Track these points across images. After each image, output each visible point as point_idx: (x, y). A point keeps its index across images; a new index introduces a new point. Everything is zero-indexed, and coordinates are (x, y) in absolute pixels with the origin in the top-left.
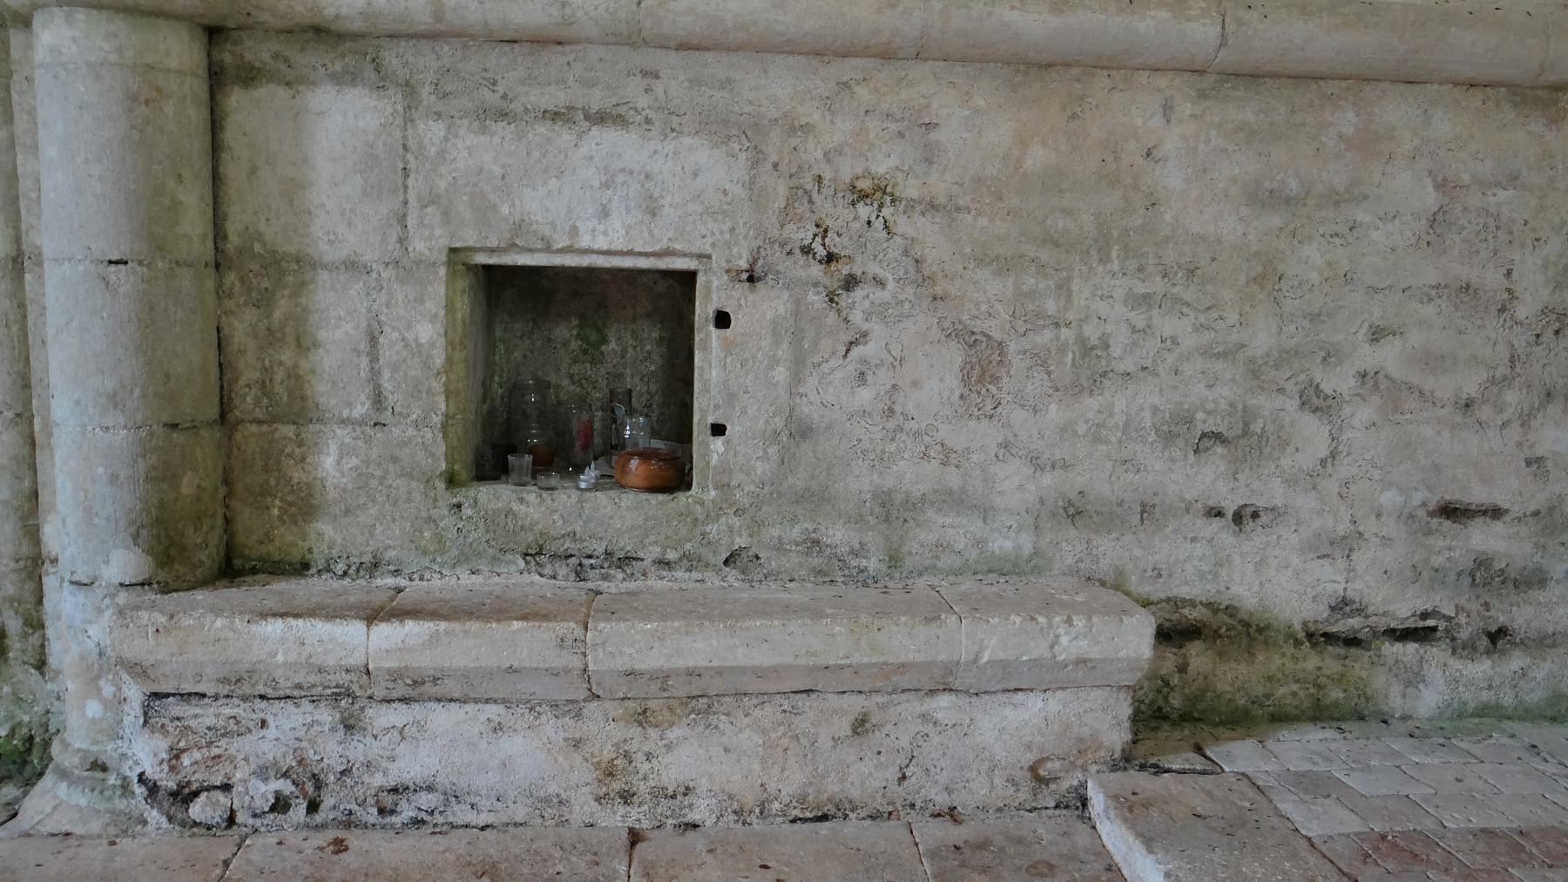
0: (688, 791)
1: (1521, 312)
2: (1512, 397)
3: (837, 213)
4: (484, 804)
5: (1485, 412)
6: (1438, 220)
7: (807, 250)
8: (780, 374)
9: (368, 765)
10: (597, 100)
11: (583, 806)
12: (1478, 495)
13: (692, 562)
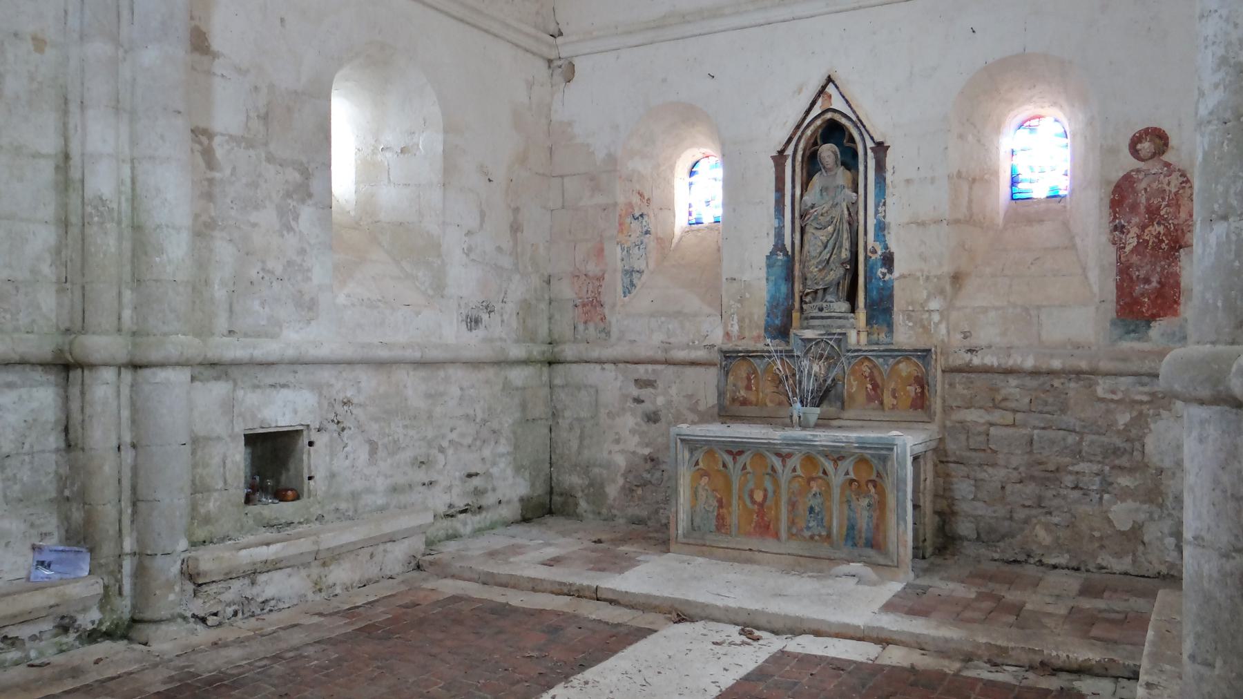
0: (335, 585)
1: (478, 420)
3: (341, 410)
4: (286, 601)
5: (473, 448)
6: (461, 398)
7: (333, 421)
8: (328, 458)
9: (257, 595)
10: (283, 381)
11: (310, 596)
12: (473, 471)
13: (307, 521)
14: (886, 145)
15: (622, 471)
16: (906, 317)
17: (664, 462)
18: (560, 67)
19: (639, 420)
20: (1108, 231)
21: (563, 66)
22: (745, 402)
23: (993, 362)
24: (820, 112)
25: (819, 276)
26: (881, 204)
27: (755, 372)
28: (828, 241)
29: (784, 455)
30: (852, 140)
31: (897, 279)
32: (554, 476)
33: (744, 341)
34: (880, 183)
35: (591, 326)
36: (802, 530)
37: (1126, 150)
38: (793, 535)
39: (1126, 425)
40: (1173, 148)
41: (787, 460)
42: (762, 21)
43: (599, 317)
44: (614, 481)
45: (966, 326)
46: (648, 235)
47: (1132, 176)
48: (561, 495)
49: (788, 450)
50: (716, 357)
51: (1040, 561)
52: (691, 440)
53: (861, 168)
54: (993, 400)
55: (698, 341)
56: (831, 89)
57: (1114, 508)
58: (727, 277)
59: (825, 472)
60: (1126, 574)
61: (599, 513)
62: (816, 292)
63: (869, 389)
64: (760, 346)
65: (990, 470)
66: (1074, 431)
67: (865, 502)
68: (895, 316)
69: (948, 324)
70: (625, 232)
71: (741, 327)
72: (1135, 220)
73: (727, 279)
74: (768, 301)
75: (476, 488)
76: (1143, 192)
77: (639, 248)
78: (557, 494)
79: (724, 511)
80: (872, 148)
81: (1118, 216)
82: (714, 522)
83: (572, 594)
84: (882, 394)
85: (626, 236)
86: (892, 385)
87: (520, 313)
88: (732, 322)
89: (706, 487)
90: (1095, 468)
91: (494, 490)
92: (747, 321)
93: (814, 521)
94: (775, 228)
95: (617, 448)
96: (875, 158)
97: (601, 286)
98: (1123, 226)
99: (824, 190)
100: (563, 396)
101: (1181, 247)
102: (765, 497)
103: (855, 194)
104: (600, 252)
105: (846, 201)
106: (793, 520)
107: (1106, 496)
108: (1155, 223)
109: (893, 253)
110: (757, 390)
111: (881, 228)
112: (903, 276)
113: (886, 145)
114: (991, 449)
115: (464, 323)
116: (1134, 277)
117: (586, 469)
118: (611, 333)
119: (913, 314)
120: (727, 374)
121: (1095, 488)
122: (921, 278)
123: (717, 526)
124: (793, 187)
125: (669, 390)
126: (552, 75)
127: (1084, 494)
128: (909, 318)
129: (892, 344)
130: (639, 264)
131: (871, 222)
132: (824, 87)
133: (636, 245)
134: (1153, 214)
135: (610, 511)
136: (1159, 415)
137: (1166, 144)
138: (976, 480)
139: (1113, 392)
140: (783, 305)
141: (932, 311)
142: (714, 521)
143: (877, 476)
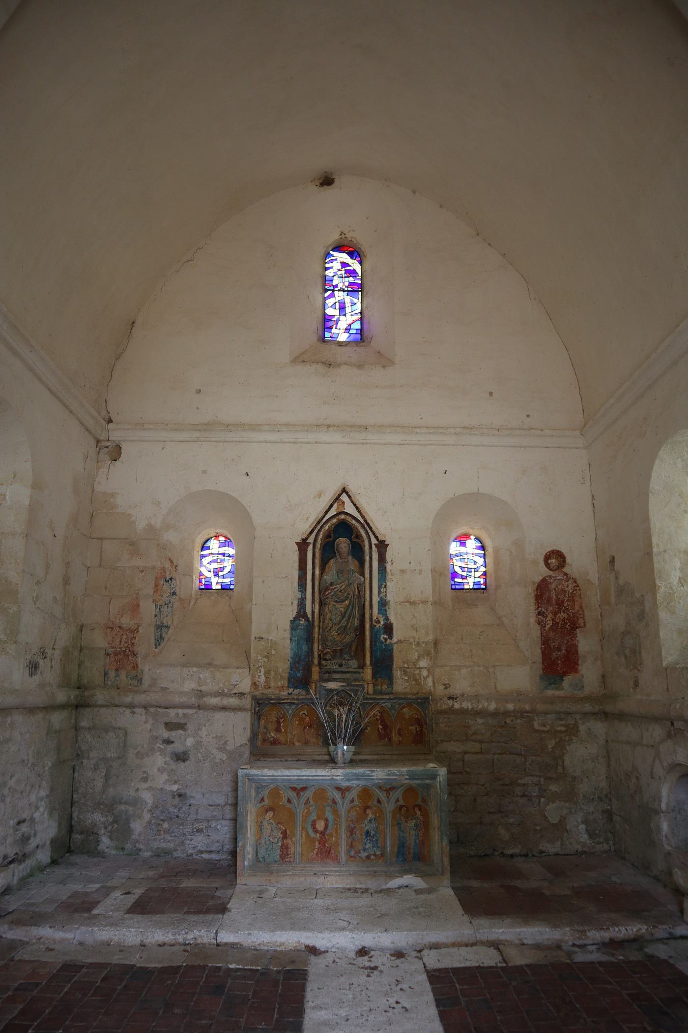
2: (28, 788)
14: (386, 543)
15: (149, 807)
16: (402, 673)
17: (191, 797)
18: (107, 447)
19: (168, 759)
20: (535, 615)
21: (110, 447)
22: (275, 742)
23: (468, 707)
24: (336, 513)
25: (338, 639)
26: (383, 586)
27: (284, 716)
28: (345, 612)
29: (344, 788)
30: (359, 536)
31: (395, 643)
32: (75, 815)
33: (270, 690)
34: (382, 570)
35: (123, 675)
36: (359, 852)
37: (542, 563)
38: (351, 857)
39: (552, 748)
40: (568, 564)
41: (347, 793)
42: (291, 440)
43: (131, 665)
44: (140, 817)
45: (446, 680)
46: (174, 596)
47: (546, 580)
48: (82, 833)
49: (347, 784)
50: (247, 702)
51: (502, 853)
52: (259, 780)
53: (367, 558)
54: (466, 734)
55: (228, 689)
56: (344, 497)
57: (548, 808)
58: (256, 636)
59: (379, 801)
60: (557, 854)
61: (123, 849)
62: (335, 652)
63: (380, 729)
64: (284, 693)
65: (466, 787)
66: (520, 754)
67: (412, 824)
68: (394, 672)
69: (433, 678)
70: (159, 592)
71: (266, 678)
72: (550, 609)
73: (255, 637)
74: (291, 658)
75: (23, 836)
76: (554, 591)
77: (168, 606)
78: (77, 833)
79: (289, 841)
80: (375, 544)
81: (540, 605)
82: (278, 852)
83: (187, 942)
84: (391, 733)
85: (159, 596)
86: (398, 726)
87: (63, 659)
88: (259, 674)
89: (271, 821)
90: (535, 779)
91: (35, 835)
92: (273, 673)
93: (370, 843)
94: (298, 599)
95: (146, 785)
96: (378, 552)
97: (135, 638)
98: (544, 612)
99: (340, 572)
100: (88, 737)
101: (577, 628)
102: (326, 826)
103: (362, 577)
104: (135, 608)
105: (357, 582)
106: (352, 844)
107: (542, 800)
108: (562, 611)
109: (392, 623)
110: (286, 731)
111: (383, 604)
112: (399, 642)
113: (386, 543)
114: (465, 771)
115: (28, 668)
116: (552, 648)
117: (110, 807)
118: (144, 680)
119: (408, 670)
120: (259, 718)
121: (535, 794)
122: (413, 643)
123: (281, 855)
124: (314, 567)
125: (199, 732)
126: (99, 452)
127: (529, 800)
128: (405, 673)
129: (392, 693)
130: (167, 621)
131: (376, 599)
132: (339, 495)
133: (166, 604)
134: (560, 604)
135: (135, 847)
136: (571, 740)
137: (564, 561)
138: (456, 796)
139: (544, 726)
140: (304, 661)
141: (422, 668)
142: (279, 850)
143: (422, 802)
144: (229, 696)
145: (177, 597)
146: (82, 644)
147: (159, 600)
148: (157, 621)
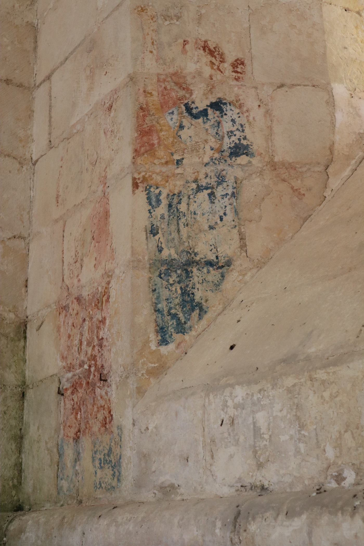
46: (243, 159)
70: (161, 153)
77: (212, 195)
133: (199, 189)
144: (342, 509)
145: (255, 161)
146: (27, 373)
147: (167, 179)
148: (160, 250)
